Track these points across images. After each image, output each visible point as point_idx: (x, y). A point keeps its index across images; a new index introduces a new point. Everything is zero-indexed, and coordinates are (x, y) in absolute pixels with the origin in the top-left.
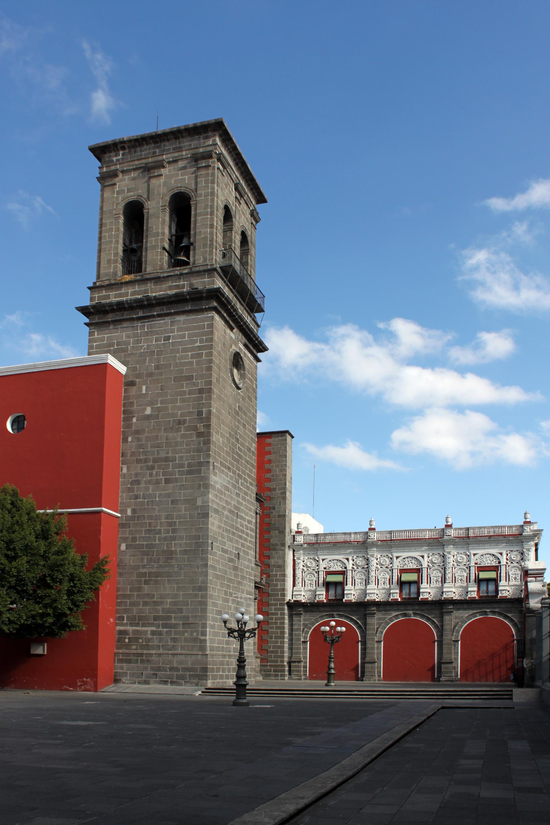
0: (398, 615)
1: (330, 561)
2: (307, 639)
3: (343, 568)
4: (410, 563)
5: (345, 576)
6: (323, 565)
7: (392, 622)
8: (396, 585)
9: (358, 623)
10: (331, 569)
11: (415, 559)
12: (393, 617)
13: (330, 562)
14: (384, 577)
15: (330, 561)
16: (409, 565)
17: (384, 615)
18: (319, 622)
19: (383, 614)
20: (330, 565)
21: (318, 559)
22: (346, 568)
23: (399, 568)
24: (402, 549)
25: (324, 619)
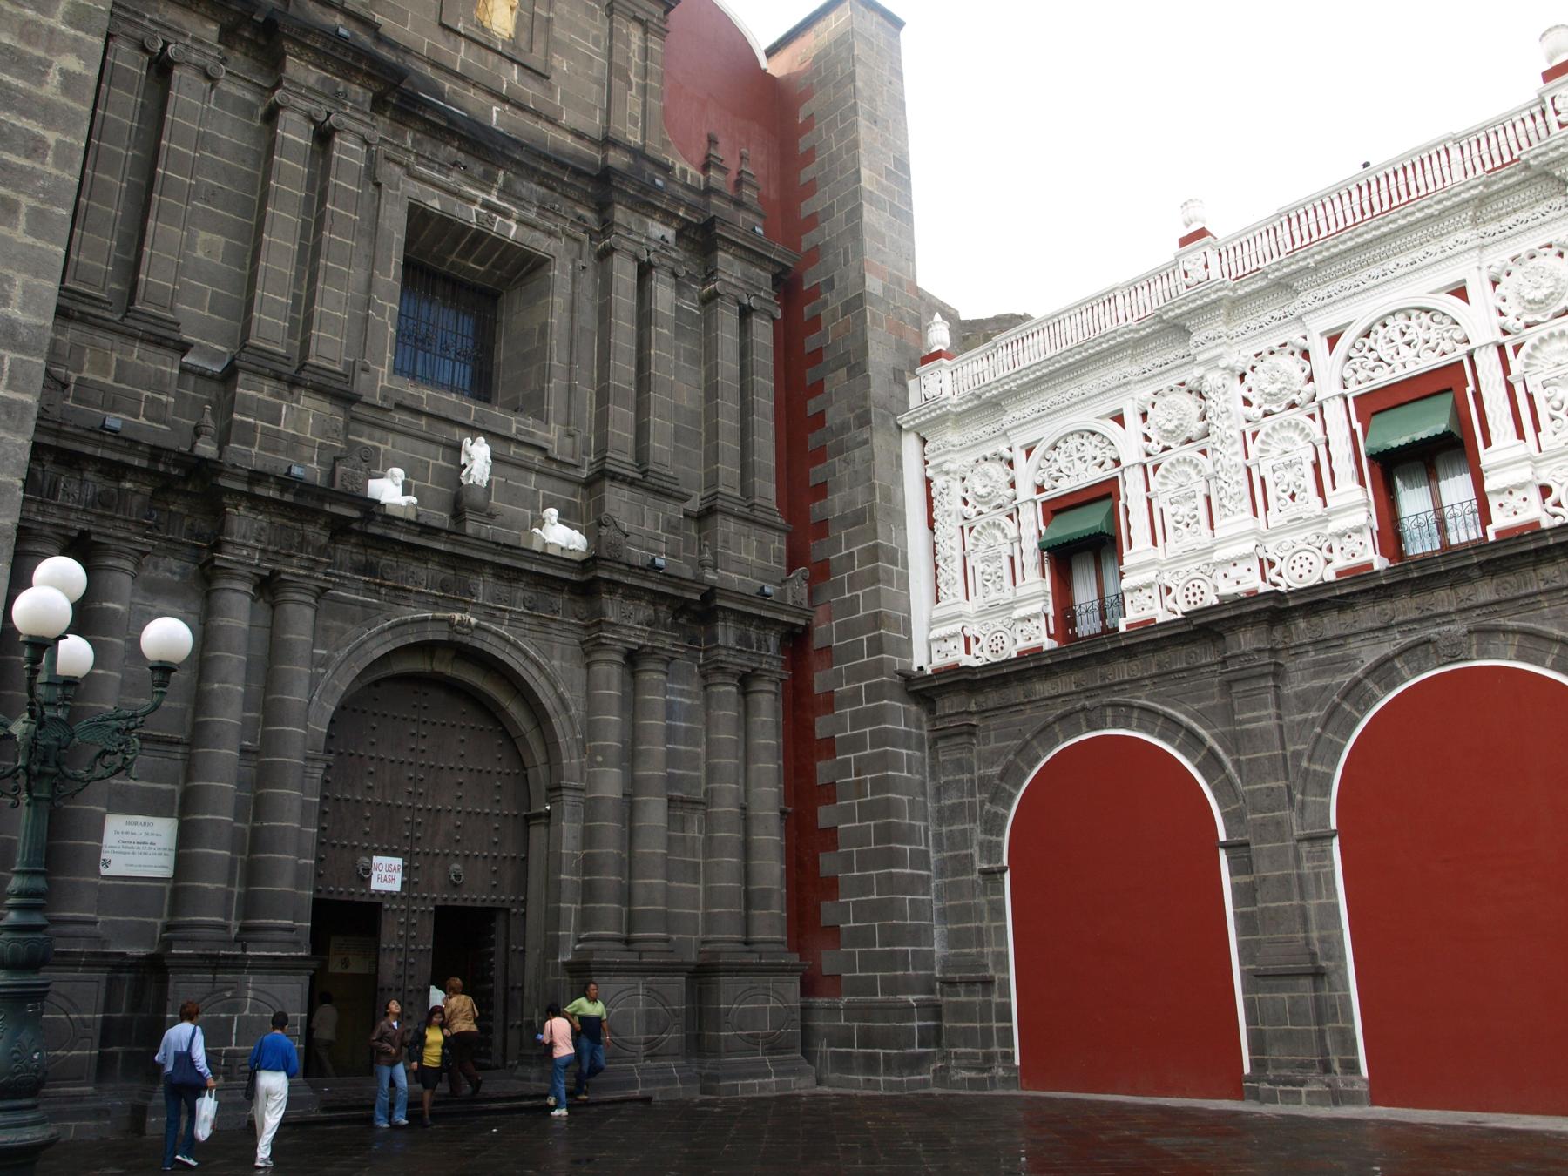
0: (1386, 661)
1: (1054, 447)
2: (1000, 859)
3: (1110, 463)
4: (1404, 350)
5: (1121, 503)
6: (1027, 474)
7: (1368, 708)
8: (1355, 485)
9: (1201, 741)
10: (1066, 486)
11: (1425, 318)
12: (1369, 673)
13: (1055, 454)
14: (1286, 459)
15: (1054, 447)
16: (1397, 362)
17: (1316, 676)
18: (1038, 759)
19: (1316, 664)
20: (1056, 466)
21: (1008, 455)
22: (1117, 462)
23: (1354, 390)
24: (1347, 282)
25: (1056, 743)
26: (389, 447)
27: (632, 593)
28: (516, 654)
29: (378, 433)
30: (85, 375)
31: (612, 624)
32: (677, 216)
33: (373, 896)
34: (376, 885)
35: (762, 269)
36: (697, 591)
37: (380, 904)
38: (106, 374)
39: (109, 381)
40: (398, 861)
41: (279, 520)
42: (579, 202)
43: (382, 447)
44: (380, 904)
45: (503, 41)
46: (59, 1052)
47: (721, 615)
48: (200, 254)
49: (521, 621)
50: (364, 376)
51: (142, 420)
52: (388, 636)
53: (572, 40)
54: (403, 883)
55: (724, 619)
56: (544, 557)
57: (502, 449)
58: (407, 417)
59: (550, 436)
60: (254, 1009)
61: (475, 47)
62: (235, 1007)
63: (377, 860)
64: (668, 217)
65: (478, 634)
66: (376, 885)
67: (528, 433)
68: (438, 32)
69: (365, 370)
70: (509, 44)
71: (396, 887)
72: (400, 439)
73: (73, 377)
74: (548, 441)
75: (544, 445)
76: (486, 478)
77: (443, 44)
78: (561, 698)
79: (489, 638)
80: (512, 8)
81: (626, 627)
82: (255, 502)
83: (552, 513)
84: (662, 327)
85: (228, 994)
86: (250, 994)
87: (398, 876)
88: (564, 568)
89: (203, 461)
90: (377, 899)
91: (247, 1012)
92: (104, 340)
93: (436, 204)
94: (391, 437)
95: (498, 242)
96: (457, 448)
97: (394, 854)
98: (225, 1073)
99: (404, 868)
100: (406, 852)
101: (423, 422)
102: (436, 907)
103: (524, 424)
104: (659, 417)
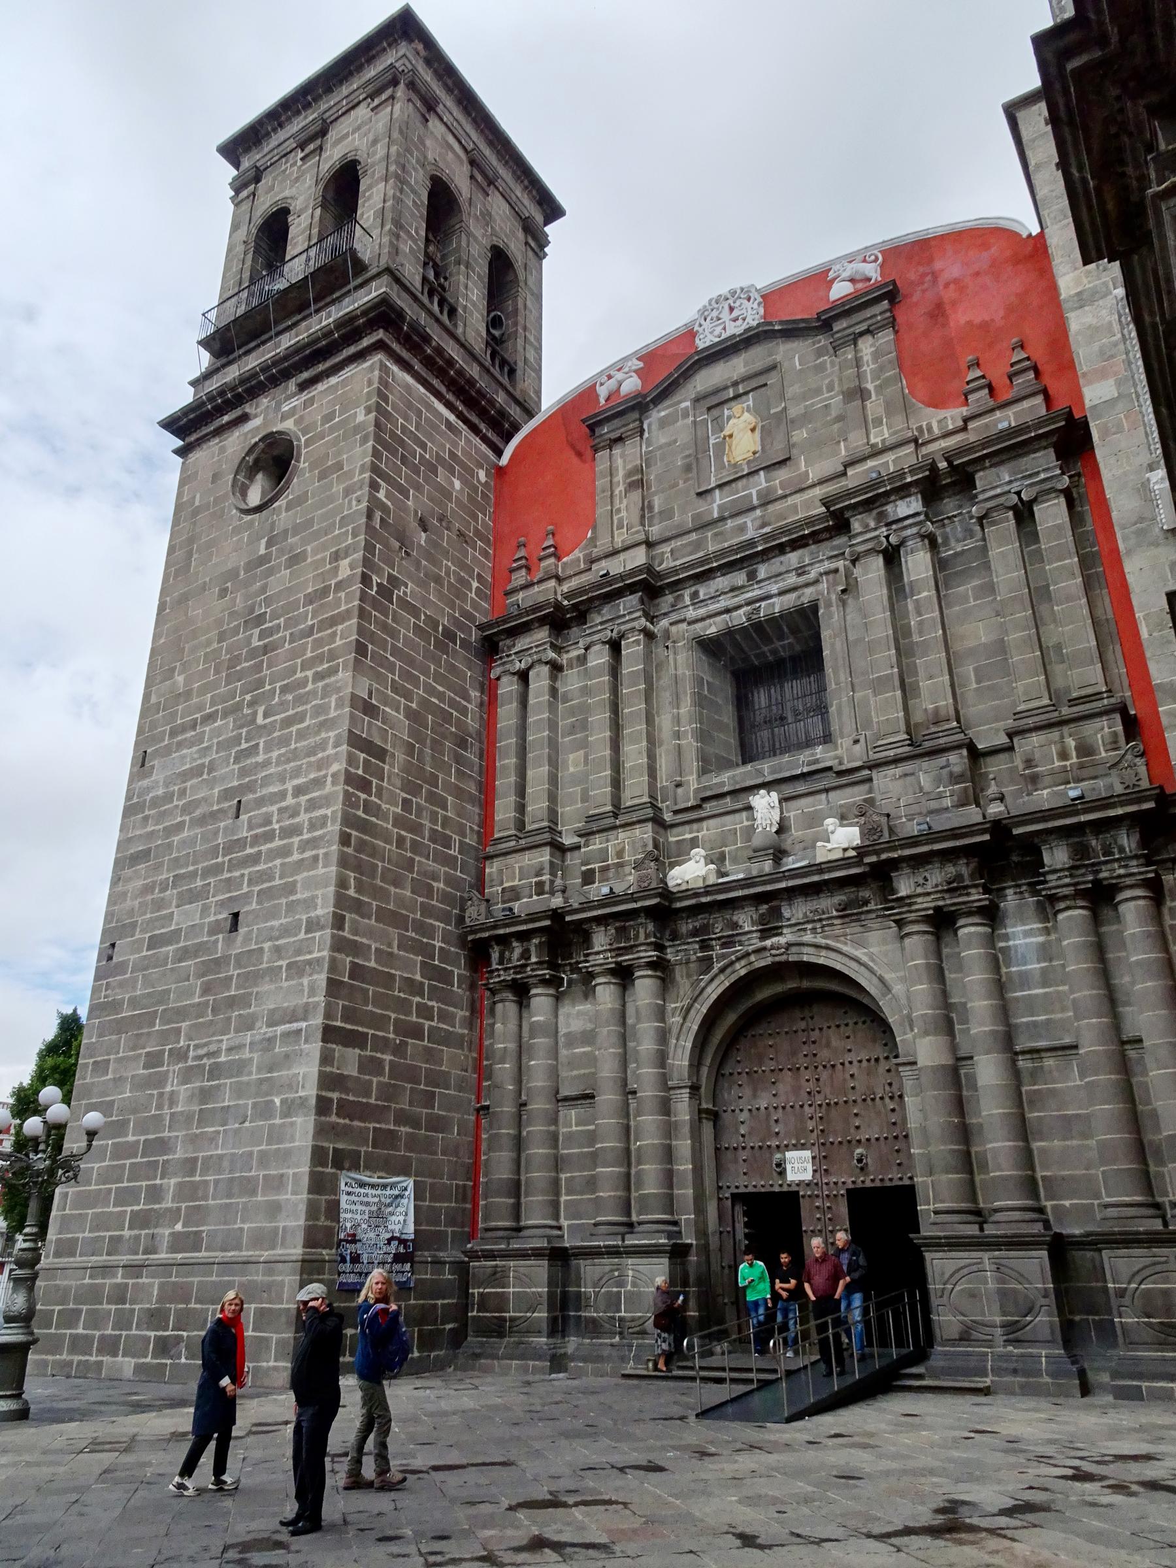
26: (705, 832)
27: (918, 862)
28: (833, 955)
29: (695, 826)
30: (506, 885)
31: (902, 899)
32: (910, 484)
33: (789, 1185)
34: (791, 1176)
35: (1035, 452)
36: (983, 832)
37: (798, 1192)
38: (513, 879)
39: (516, 883)
40: (807, 1154)
41: (617, 924)
42: (831, 538)
43: (700, 835)
44: (798, 1192)
45: (749, 462)
46: (529, 1314)
47: (1036, 840)
48: (572, 769)
49: (833, 925)
50: (680, 790)
51: (535, 897)
52: (722, 977)
53: (806, 407)
54: (815, 1171)
55: (1045, 842)
56: (832, 865)
57: (789, 790)
58: (714, 803)
59: (839, 752)
60: (634, 1285)
61: (727, 488)
62: (621, 1284)
63: (789, 1154)
64: (902, 491)
65: (794, 949)
66: (791, 1176)
67: (817, 761)
68: (700, 502)
69: (678, 785)
70: (755, 460)
71: (808, 1176)
72: (712, 822)
73: (500, 889)
74: (836, 757)
75: (828, 764)
76: (776, 817)
77: (701, 506)
78: (881, 979)
79: (806, 950)
80: (753, 430)
81: (919, 895)
82: (601, 920)
83: (831, 823)
84: (919, 593)
85: (616, 1274)
86: (630, 1273)
87: (810, 1168)
88: (849, 866)
89: (555, 911)
90: (794, 1188)
91: (629, 1287)
92: (511, 860)
93: (713, 630)
94: (705, 824)
95: (773, 620)
96: (749, 808)
97: (803, 1147)
98: (621, 1333)
99: (814, 1158)
100: (813, 1144)
101: (728, 799)
102: (848, 1190)
103: (813, 755)
104: (931, 678)
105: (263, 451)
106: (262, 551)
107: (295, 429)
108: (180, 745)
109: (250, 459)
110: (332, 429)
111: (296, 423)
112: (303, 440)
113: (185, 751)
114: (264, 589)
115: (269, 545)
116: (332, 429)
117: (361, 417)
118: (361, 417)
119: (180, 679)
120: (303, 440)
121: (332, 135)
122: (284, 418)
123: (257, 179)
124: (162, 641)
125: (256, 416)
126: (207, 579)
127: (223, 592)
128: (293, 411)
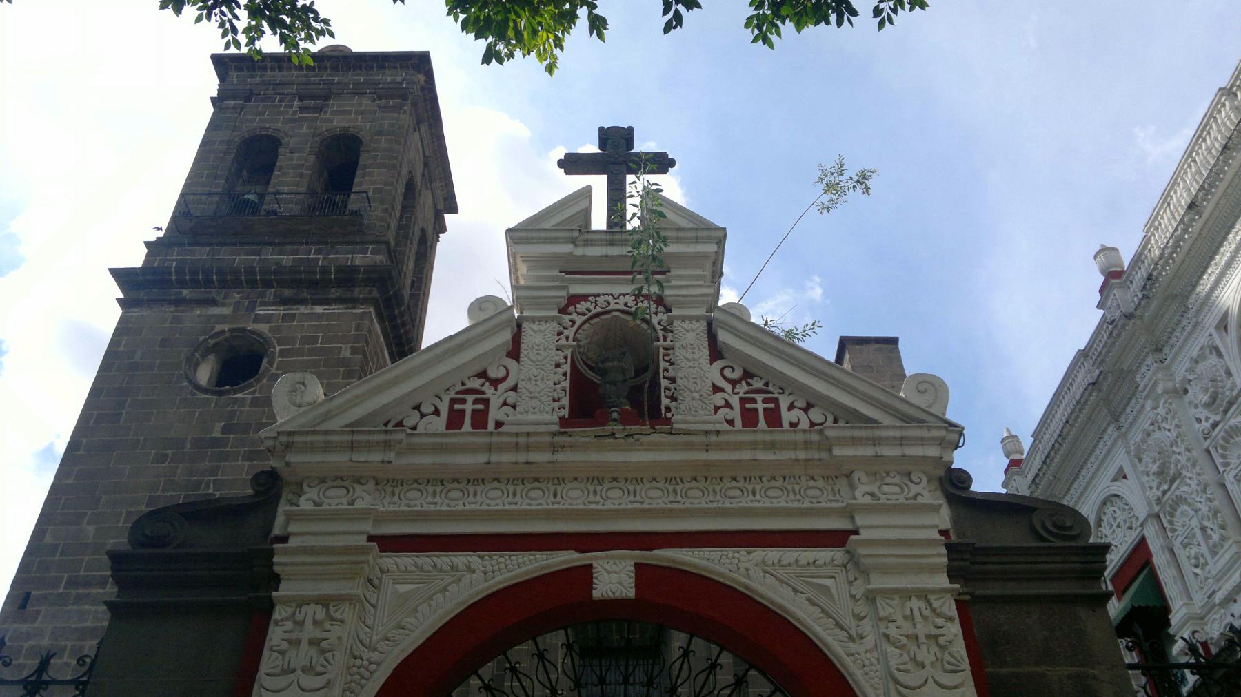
105: (226, 340)
106: (217, 434)
107: (270, 335)
108: (79, 599)
109: (212, 342)
110: (312, 352)
111: (271, 329)
112: (278, 348)
113: (87, 607)
114: (213, 471)
115: (225, 430)
116: (312, 352)
117: (346, 353)
118: (346, 353)
119: (91, 529)
120: (278, 348)
121: (334, 104)
122: (257, 319)
123: (248, 99)
124: (70, 481)
125: (223, 305)
126: (142, 438)
127: (161, 458)
128: (267, 319)
